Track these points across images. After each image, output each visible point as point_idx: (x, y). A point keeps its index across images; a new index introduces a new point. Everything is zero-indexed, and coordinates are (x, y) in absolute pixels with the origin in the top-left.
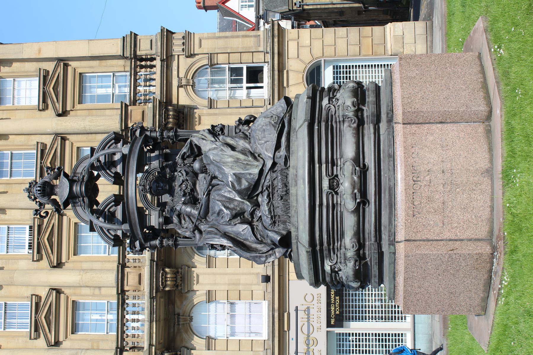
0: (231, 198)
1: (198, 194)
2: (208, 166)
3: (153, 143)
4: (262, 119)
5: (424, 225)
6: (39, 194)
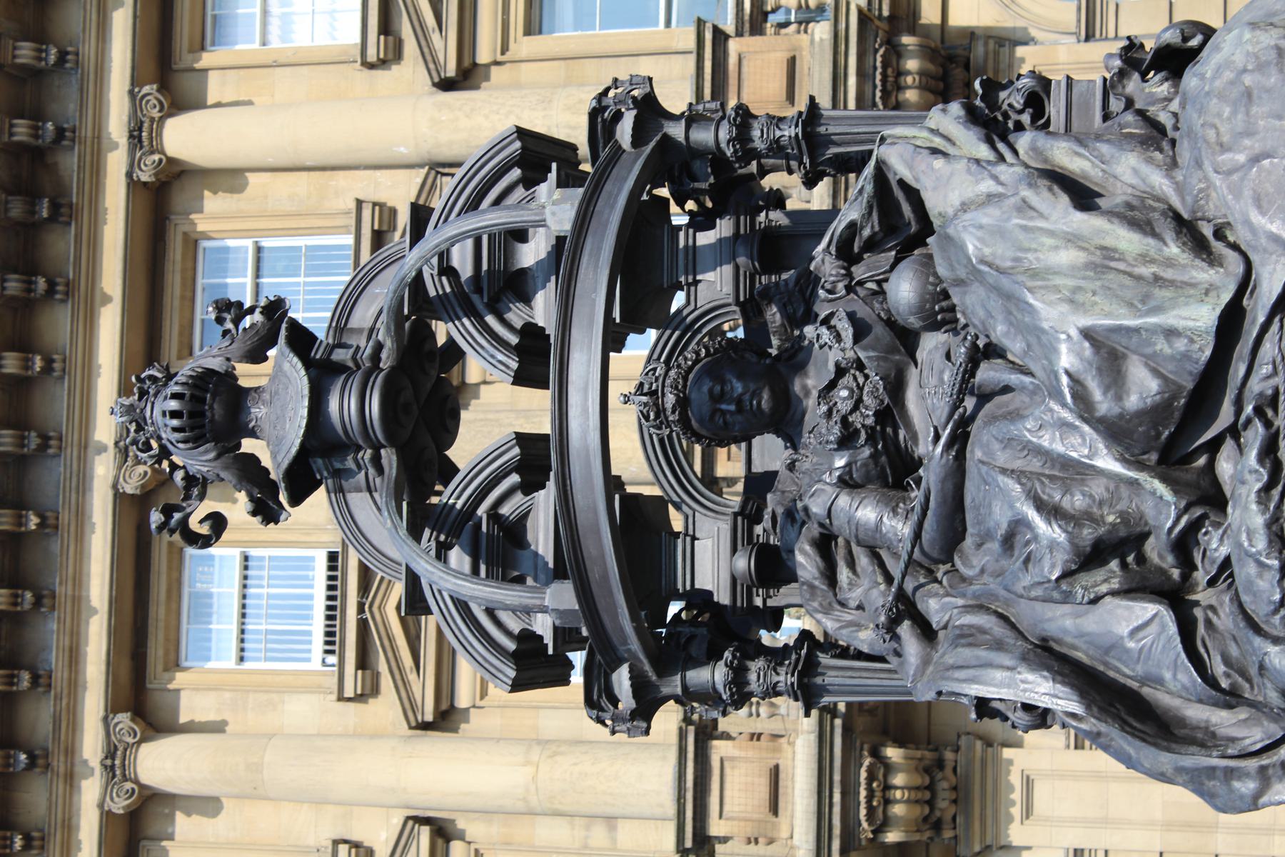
0: (1072, 459)
1: (914, 437)
2: (957, 289)
3: (712, 180)
4: (1240, 36)
6: (175, 430)
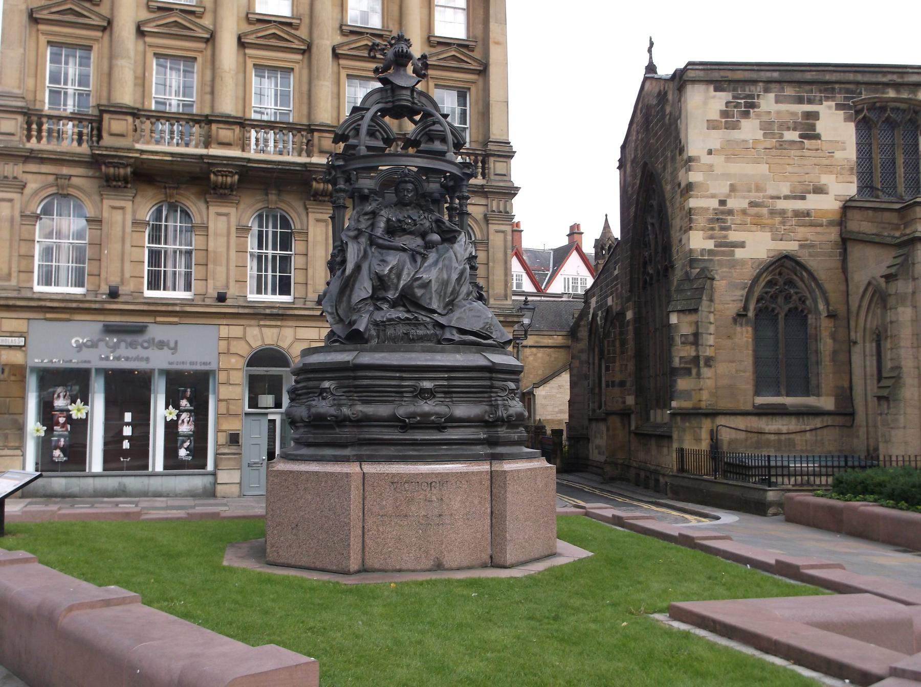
1: (400, 237)
5: (381, 494)
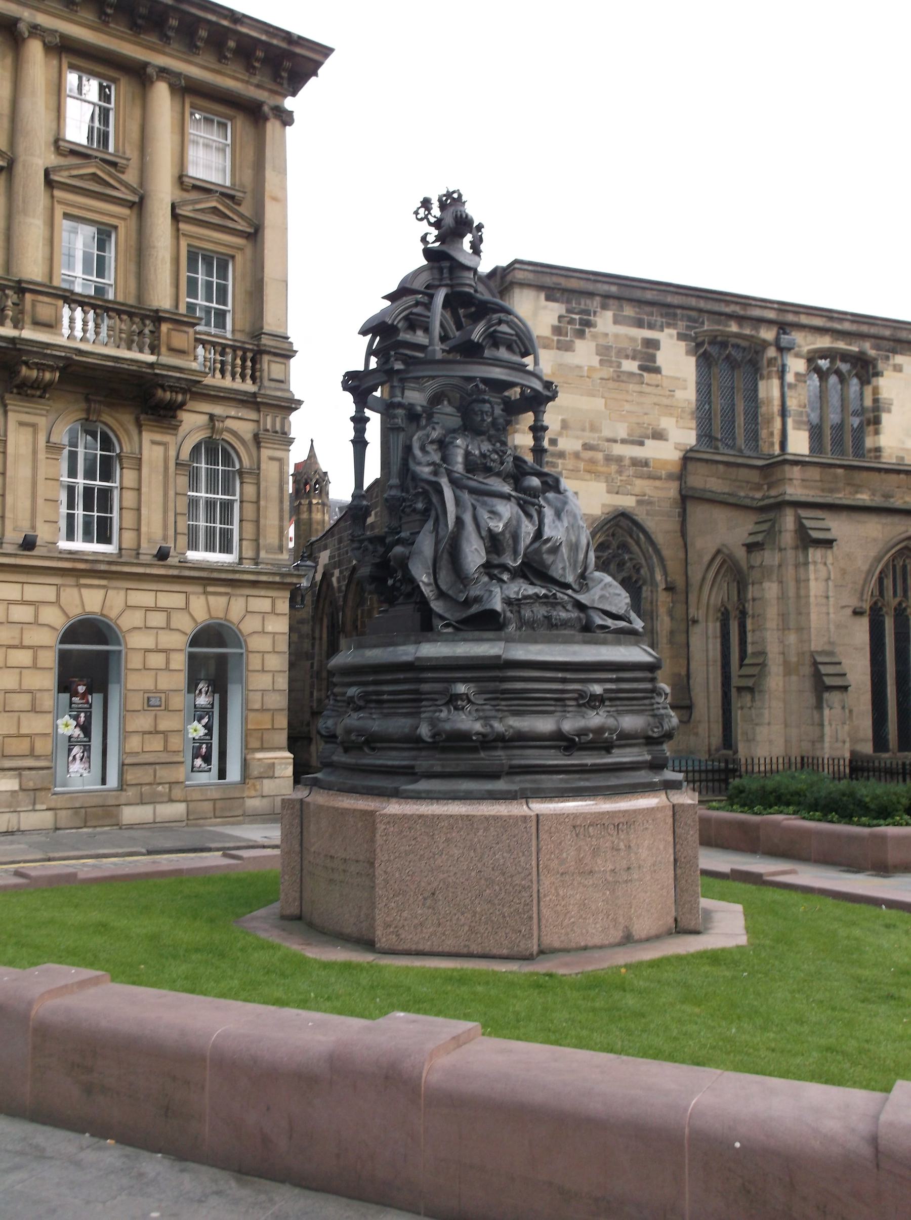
5: (560, 843)
